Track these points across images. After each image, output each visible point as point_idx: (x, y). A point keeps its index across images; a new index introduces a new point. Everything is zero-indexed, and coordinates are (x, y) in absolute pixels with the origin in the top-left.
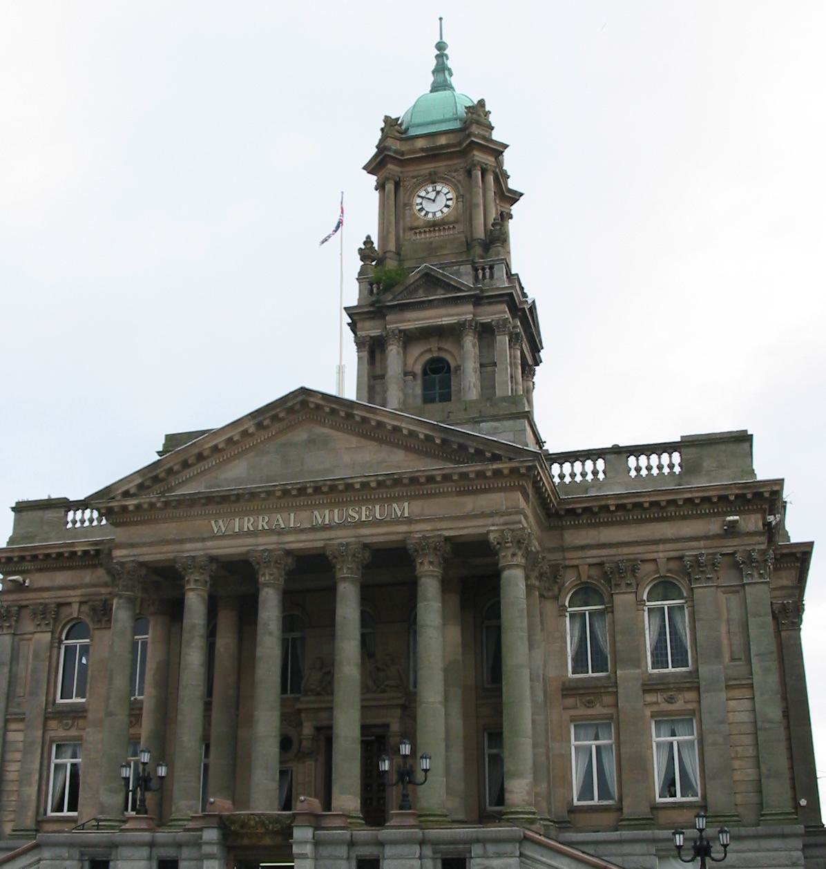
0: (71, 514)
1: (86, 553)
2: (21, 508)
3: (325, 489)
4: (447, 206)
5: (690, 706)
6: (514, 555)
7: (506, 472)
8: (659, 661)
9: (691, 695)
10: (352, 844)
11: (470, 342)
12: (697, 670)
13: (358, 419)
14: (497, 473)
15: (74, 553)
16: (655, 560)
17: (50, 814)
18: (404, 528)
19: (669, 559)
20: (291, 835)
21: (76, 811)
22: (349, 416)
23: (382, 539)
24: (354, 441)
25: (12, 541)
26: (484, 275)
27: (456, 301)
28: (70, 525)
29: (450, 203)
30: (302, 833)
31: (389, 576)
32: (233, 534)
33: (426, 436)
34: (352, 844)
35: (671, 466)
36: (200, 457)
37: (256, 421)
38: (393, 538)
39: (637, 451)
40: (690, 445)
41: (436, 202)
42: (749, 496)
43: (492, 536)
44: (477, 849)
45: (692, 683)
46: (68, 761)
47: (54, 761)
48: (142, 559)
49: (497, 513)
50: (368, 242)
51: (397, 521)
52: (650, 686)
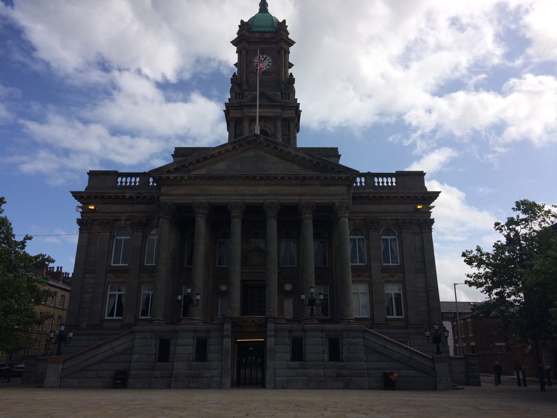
0: (119, 179)
1: (131, 197)
2: (92, 174)
3: (265, 178)
4: (268, 65)
5: (400, 279)
6: (345, 212)
7: (344, 178)
9: (400, 275)
10: (290, 331)
12: (403, 264)
13: (279, 150)
14: (340, 178)
15: (125, 197)
16: (386, 220)
17: (106, 318)
18: (298, 198)
19: (392, 220)
20: (266, 327)
21: (121, 316)
22: (275, 148)
23: (288, 202)
25: (87, 188)
26: (285, 97)
27: (274, 106)
28: (119, 184)
29: (270, 64)
30: (271, 326)
33: (309, 160)
34: (290, 331)
35: (392, 183)
36: (205, 159)
37: (233, 146)
38: (293, 201)
39: (379, 175)
40: (399, 175)
42: (426, 197)
43: (336, 204)
45: (401, 269)
46: (117, 293)
47: (109, 293)
48: (175, 202)
49: (334, 194)
52: (385, 270)
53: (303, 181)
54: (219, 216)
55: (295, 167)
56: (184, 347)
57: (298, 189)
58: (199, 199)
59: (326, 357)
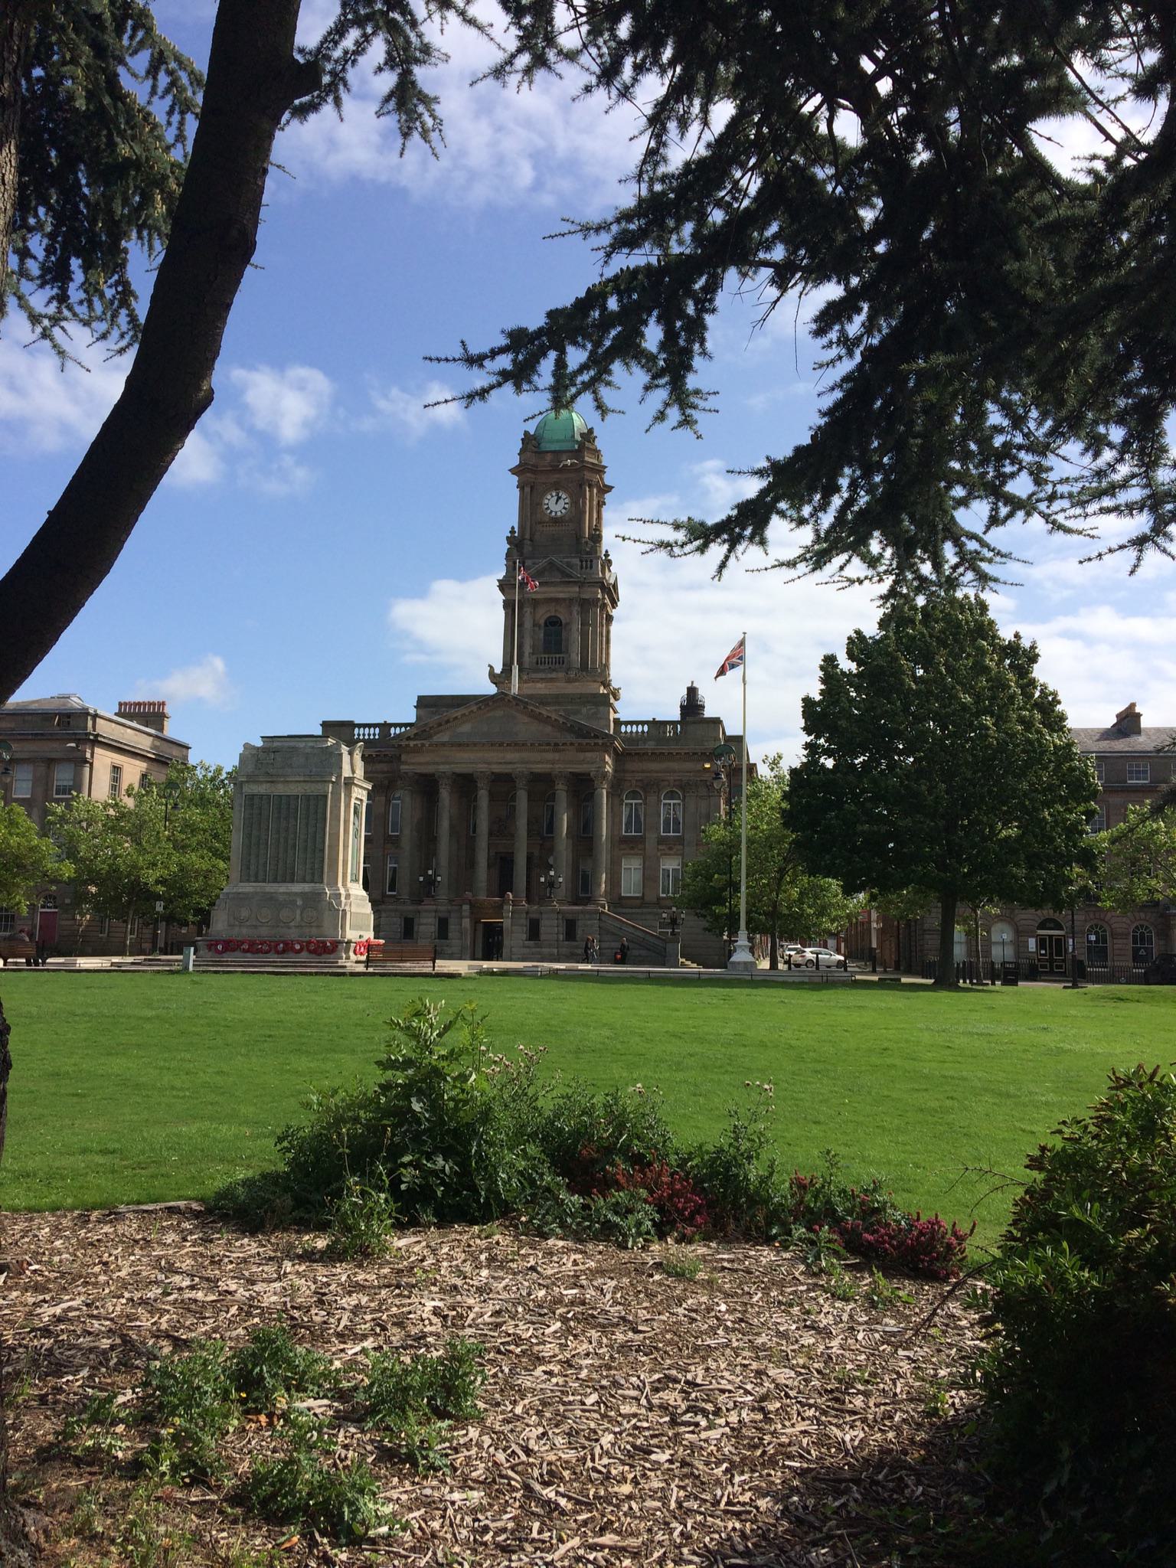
8: (667, 830)
11: (576, 609)
24: (526, 719)
31: (541, 785)
32: (466, 761)
41: (556, 505)
44: (581, 916)
45: (680, 840)
50: (512, 531)
51: (548, 762)
52: (661, 841)
53: (556, 747)
54: (465, 784)
55: (548, 729)
56: (427, 926)
57: (550, 756)
58: (443, 768)
59: (561, 937)
